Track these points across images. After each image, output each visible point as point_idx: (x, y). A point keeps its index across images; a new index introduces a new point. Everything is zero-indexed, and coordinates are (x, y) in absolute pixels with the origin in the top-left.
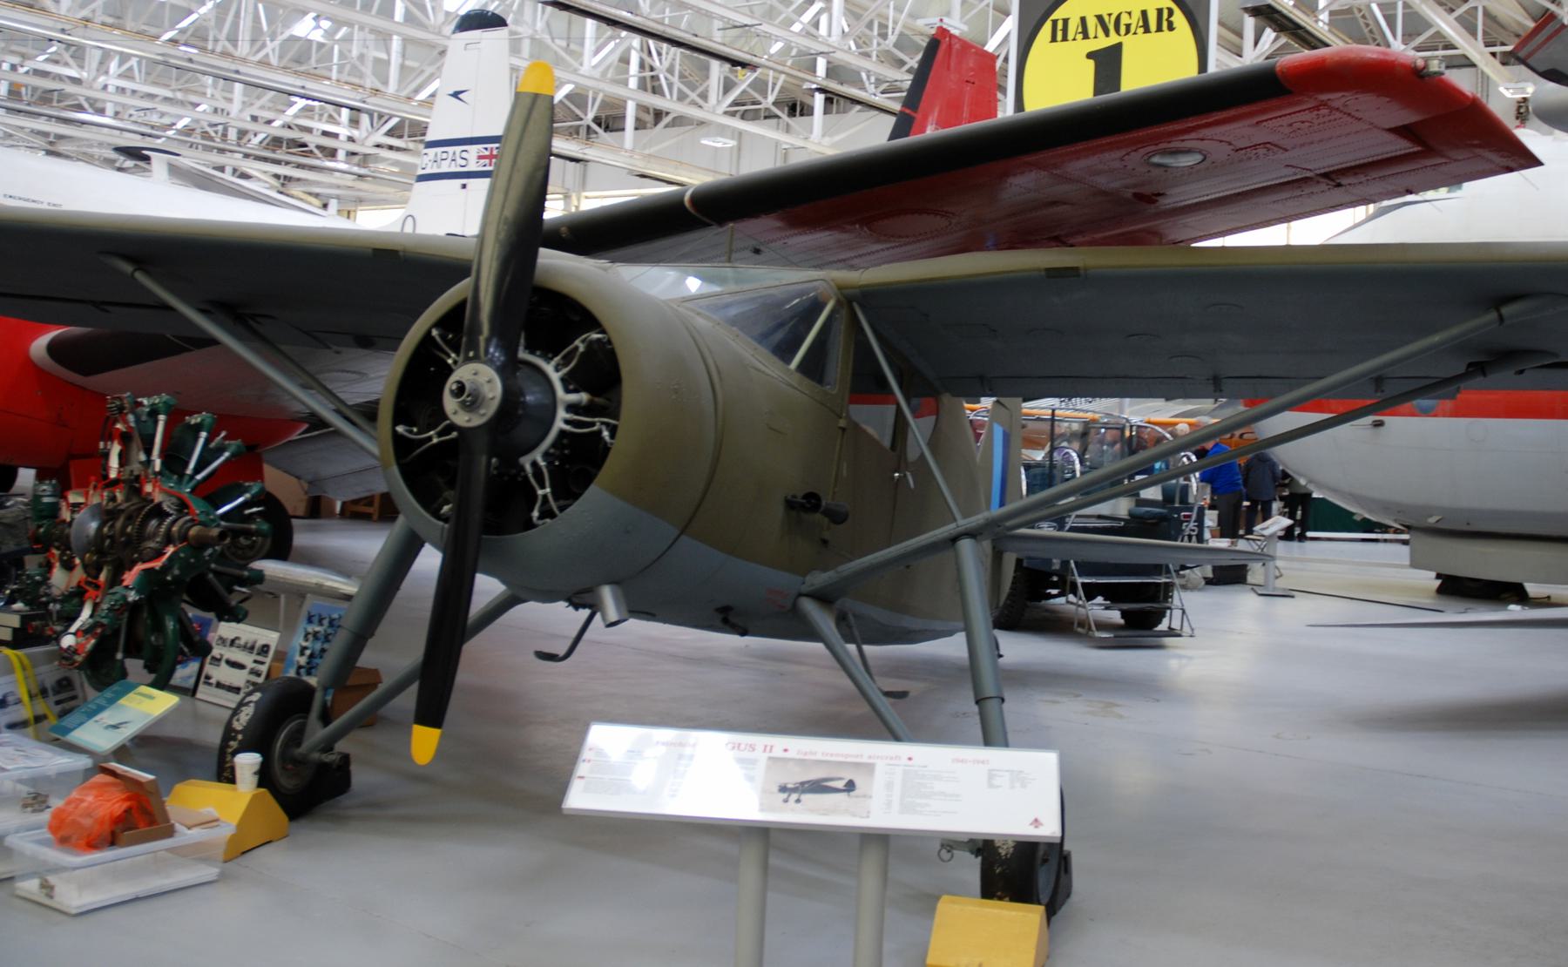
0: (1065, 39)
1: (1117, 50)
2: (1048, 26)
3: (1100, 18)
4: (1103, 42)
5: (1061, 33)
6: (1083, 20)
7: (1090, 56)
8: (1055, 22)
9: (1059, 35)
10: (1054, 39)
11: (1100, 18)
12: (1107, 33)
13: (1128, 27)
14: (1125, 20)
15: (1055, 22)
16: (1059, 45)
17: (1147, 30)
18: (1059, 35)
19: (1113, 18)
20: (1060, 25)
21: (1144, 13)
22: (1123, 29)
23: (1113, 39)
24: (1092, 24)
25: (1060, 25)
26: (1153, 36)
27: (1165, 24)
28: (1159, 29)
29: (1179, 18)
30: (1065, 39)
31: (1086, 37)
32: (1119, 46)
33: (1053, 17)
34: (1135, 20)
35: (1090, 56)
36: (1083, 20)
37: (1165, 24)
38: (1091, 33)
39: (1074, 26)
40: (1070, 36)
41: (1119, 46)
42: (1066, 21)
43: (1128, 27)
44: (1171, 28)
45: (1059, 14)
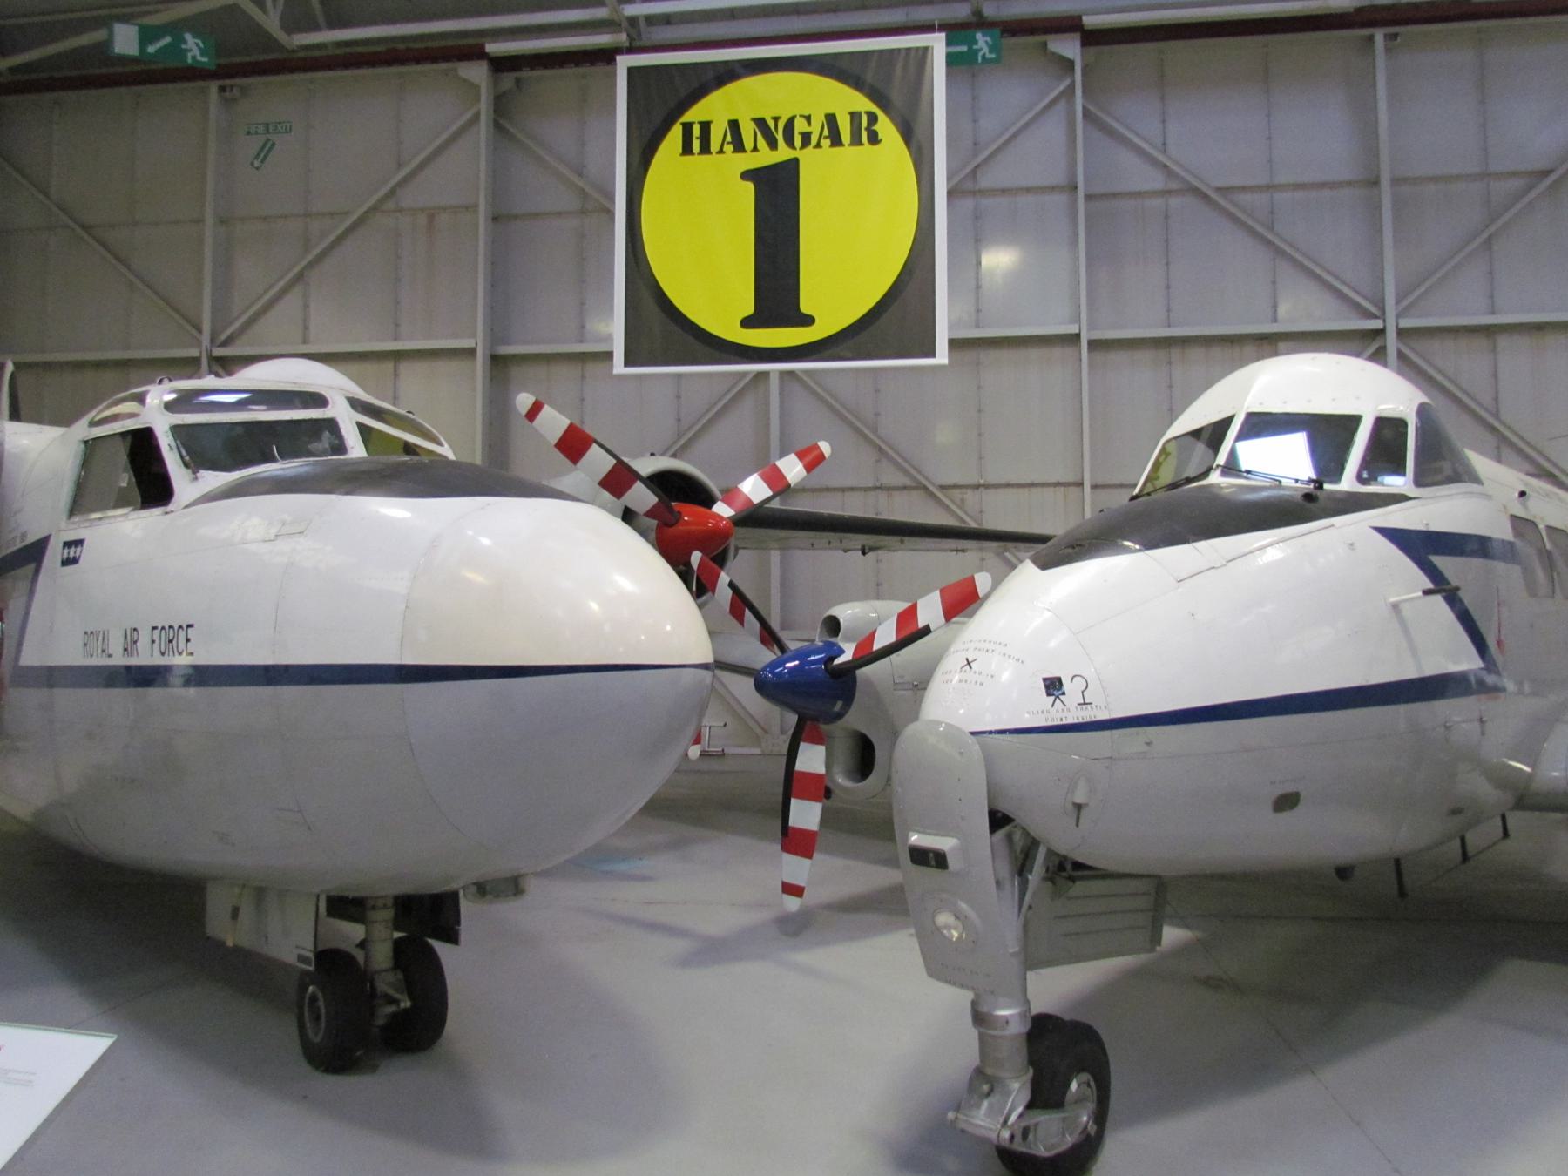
0: (705, 149)
1: (790, 169)
2: (676, 132)
3: (760, 123)
4: (766, 157)
5: (698, 141)
6: (734, 125)
7: (746, 175)
8: (688, 128)
10: (687, 149)
11: (760, 123)
12: (773, 144)
14: (800, 126)
15: (688, 128)
16: (697, 160)
17: (836, 141)
20: (696, 131)
21: (831, 119)
22: (798, 141)
23: (783, 153)
24: (748, 131)
25: (696, 131)
26: (847, 151)
27: (864, 135)
29: (885, 127)
30: (705, 149)
31: (739, 146)
32: (794, 163)
33: (686, 118)
35: (746, 175)
36: (734, 125)
37: (864, 135)
38: (748, 144)
40: (715, 146)
41: (796, 161)
42: (706, 126)
43: (806, 137)
44: (874, 139)
45: (694, 115)
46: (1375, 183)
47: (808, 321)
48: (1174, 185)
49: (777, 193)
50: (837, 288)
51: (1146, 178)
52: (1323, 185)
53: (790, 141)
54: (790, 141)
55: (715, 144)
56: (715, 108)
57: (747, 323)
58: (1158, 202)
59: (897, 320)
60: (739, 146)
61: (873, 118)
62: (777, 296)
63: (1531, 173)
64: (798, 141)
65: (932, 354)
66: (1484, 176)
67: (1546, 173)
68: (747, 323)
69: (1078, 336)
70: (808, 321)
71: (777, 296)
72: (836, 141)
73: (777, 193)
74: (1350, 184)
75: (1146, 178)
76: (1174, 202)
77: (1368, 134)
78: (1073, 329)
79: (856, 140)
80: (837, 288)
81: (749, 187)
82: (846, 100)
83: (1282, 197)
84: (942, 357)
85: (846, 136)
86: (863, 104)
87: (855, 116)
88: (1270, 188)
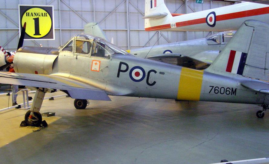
0: (29, 16)
3: (35, 13)
5: (28, 15)
6: (32, 13)
8: (27, 13)
9: (28, 15)
10: (27, 16)
11: (35, 13)
12: (36, 16)
13: (40, 15)
14: (39, 14)
17: (43, 16)
18: (28, 15)
19: (37, 13)
20: (28, 14)
22: (39, 15)
23: (37, 17)
24: (33, 14)
25: (28, 14)
26: (44, 17)
28: (45, 16)
29: (48, 15)
31: (32, 16)
32: (38, 18)
34: (40, 14)
36: (32, 13)
38: (33, 15)
39: (30, 14)
41: (38, 18)
42: (29, 13)
43: (40, 15)
44: (47, 16)
45: (28, 12)
46: (93, 12)
47: (40, 35)
48: (71, 10)
49: (37, 21)
50: (44, 31)
51: (68, 9)
52: (88, 11)
53: (38, 15)
54: (38, 15)
55: (30, 15)
56: (30, 11)
57: (34, 35)
58: (69, 12)
59: (49, 35)
60: (32, 16)
61: (46, 14)
62: (37, 32)
63: (109, 12)
64: (39, 15)
65: (53, 38)
66: (105, 12)
67: (111, 12)
68: (34, 35)
69: (60, 30)
70: (40, 35)
71: (37, 32)
72: (43, 16)
73: (37, 21)
74: (89, 11)
75: (68, 9)
76: (71, 12)
77: (92, 5)
78: (59, 29)
79: (45, 16)
80: (44, 31)
81: (34, 20)
82: (44, 12)
83: (83, 12)
84: (54, 39)
85: (44, 15)
86: (46, 12)
87: (45, 13)
88: (82, 11)
